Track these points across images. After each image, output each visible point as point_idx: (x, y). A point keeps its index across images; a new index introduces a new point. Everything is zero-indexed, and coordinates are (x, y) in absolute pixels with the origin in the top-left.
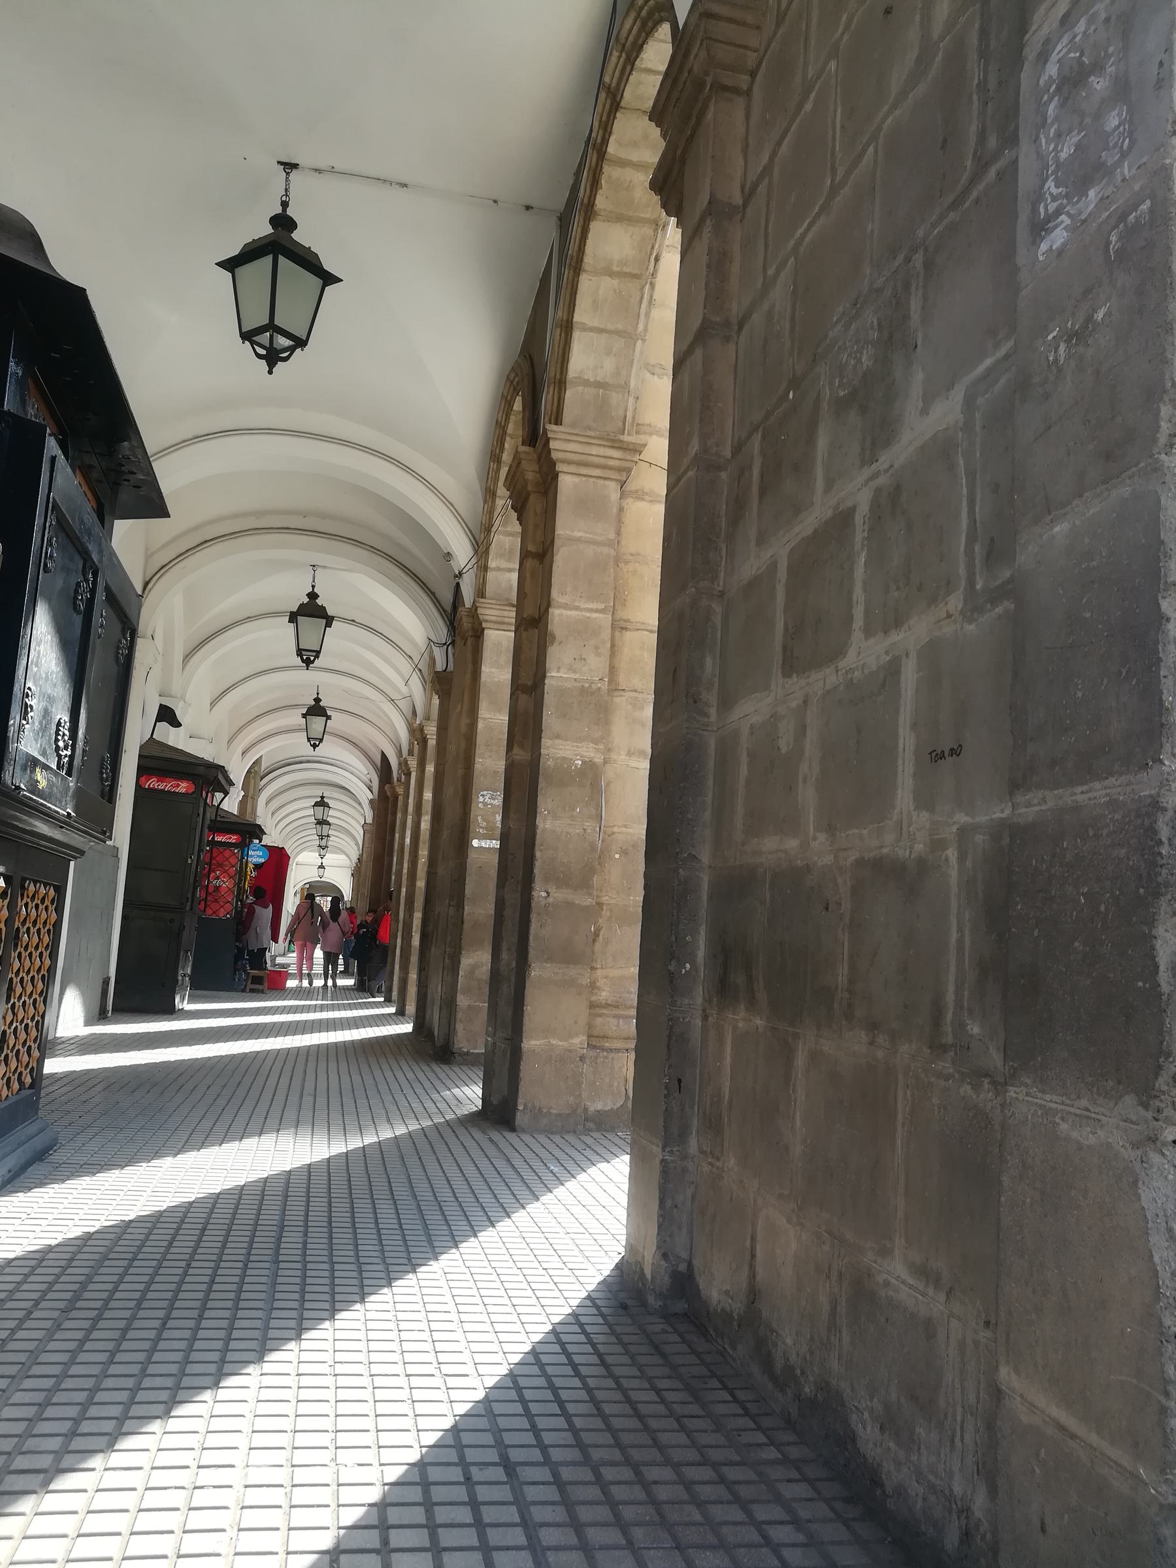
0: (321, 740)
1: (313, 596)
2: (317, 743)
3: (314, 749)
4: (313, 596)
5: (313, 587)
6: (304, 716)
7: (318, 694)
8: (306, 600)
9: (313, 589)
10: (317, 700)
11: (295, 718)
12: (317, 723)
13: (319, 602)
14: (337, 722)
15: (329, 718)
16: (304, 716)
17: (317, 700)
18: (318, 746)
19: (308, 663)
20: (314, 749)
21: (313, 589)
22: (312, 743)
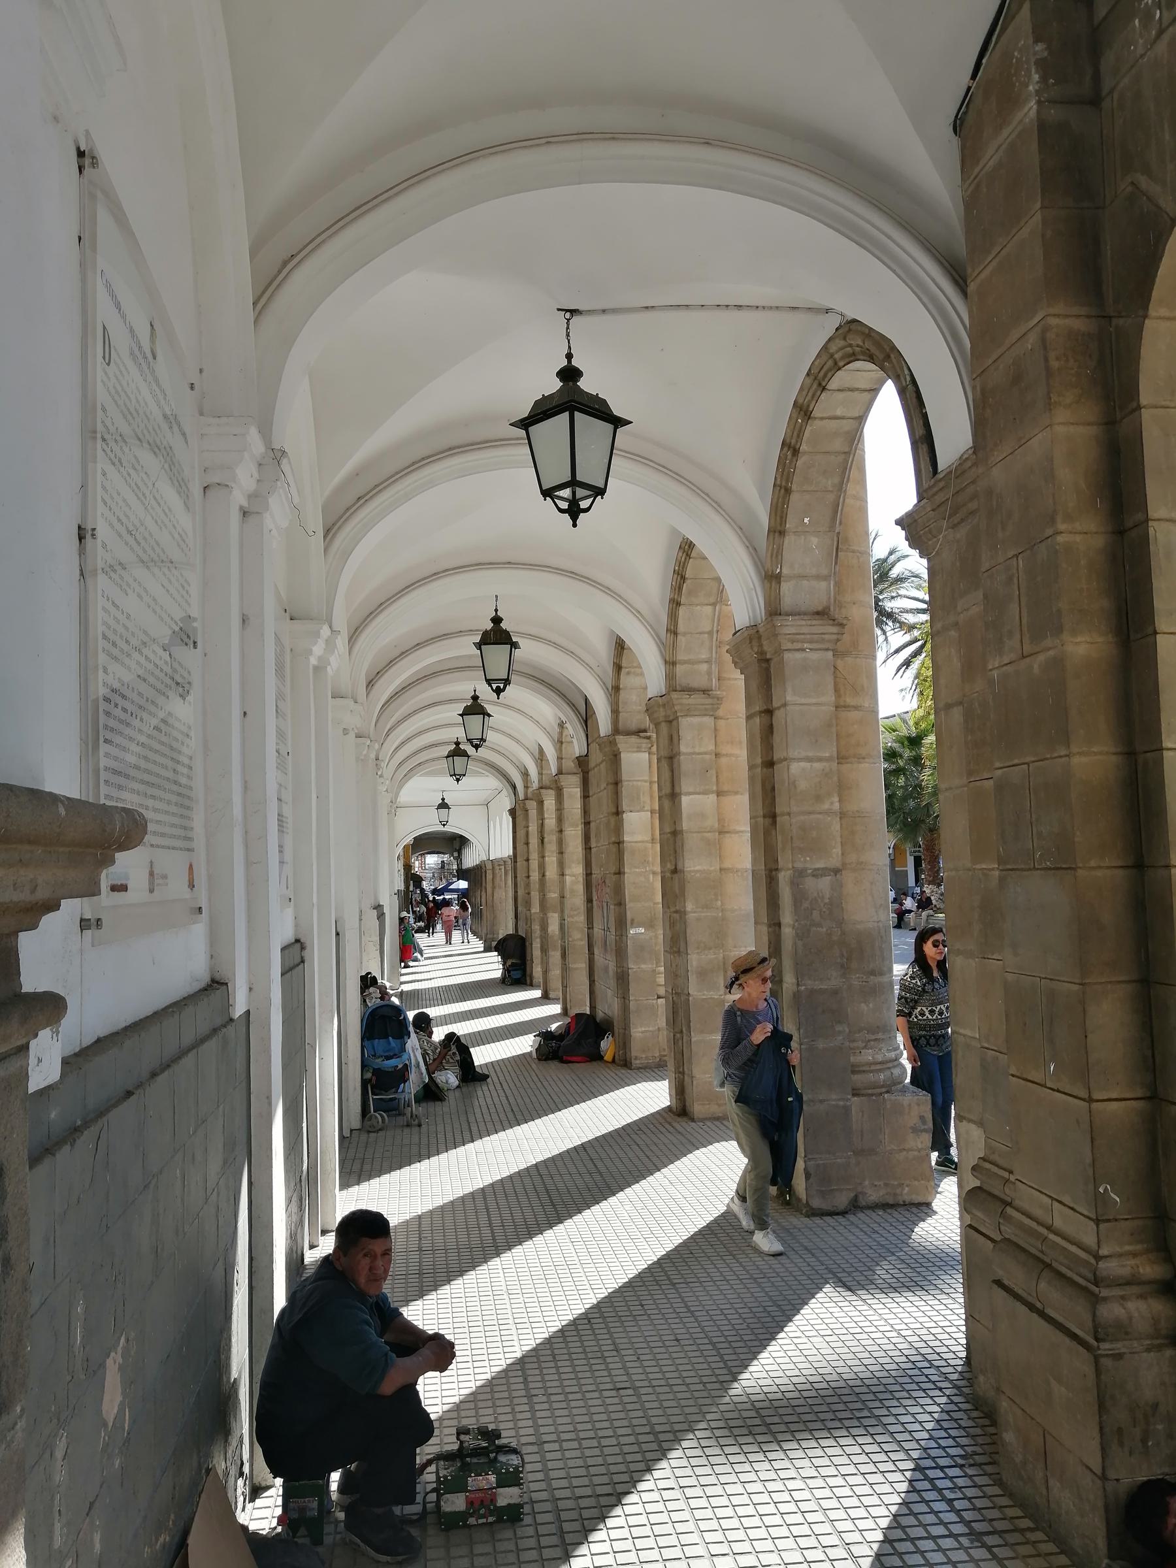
0: (507, 682)
1: (569, 374)
2: (502, 686)
3: (498, 695)
4: (569, 374)
5: (569, 356)
6: (479, 646)
7: (496, 610)
8: (556, 385)
9: (569, 361)
10: (497, 620)
11: (466, 647)
12: (497, 654)
13: (584, 384)
14: (527, 651)
15: (514, 645)
16: (479, 646)
17: (497, 620)
18: (503, 690)
19: (574, 511)
20: (498, 695)
21: (569, 361)
22: (494, 686)
